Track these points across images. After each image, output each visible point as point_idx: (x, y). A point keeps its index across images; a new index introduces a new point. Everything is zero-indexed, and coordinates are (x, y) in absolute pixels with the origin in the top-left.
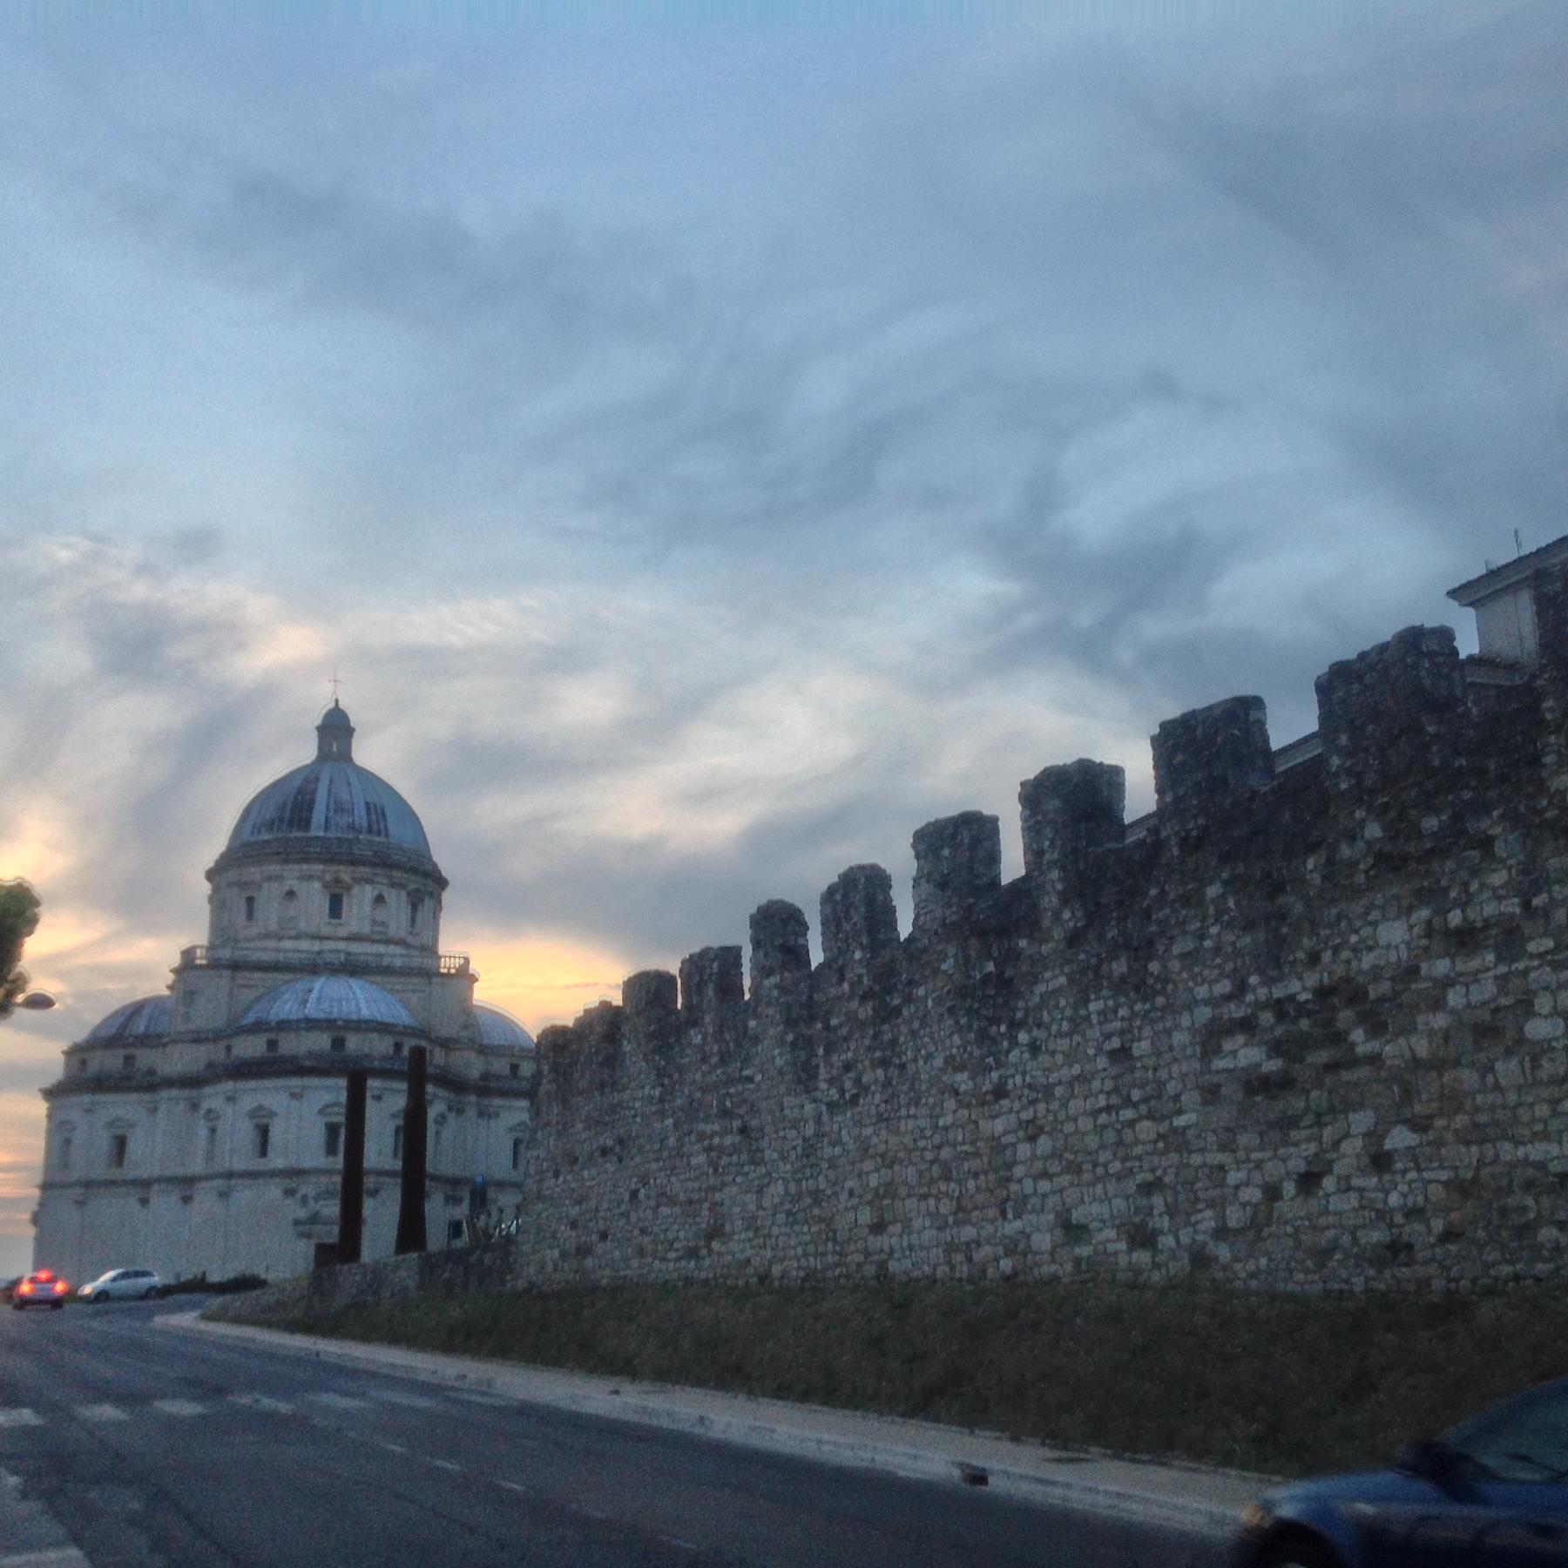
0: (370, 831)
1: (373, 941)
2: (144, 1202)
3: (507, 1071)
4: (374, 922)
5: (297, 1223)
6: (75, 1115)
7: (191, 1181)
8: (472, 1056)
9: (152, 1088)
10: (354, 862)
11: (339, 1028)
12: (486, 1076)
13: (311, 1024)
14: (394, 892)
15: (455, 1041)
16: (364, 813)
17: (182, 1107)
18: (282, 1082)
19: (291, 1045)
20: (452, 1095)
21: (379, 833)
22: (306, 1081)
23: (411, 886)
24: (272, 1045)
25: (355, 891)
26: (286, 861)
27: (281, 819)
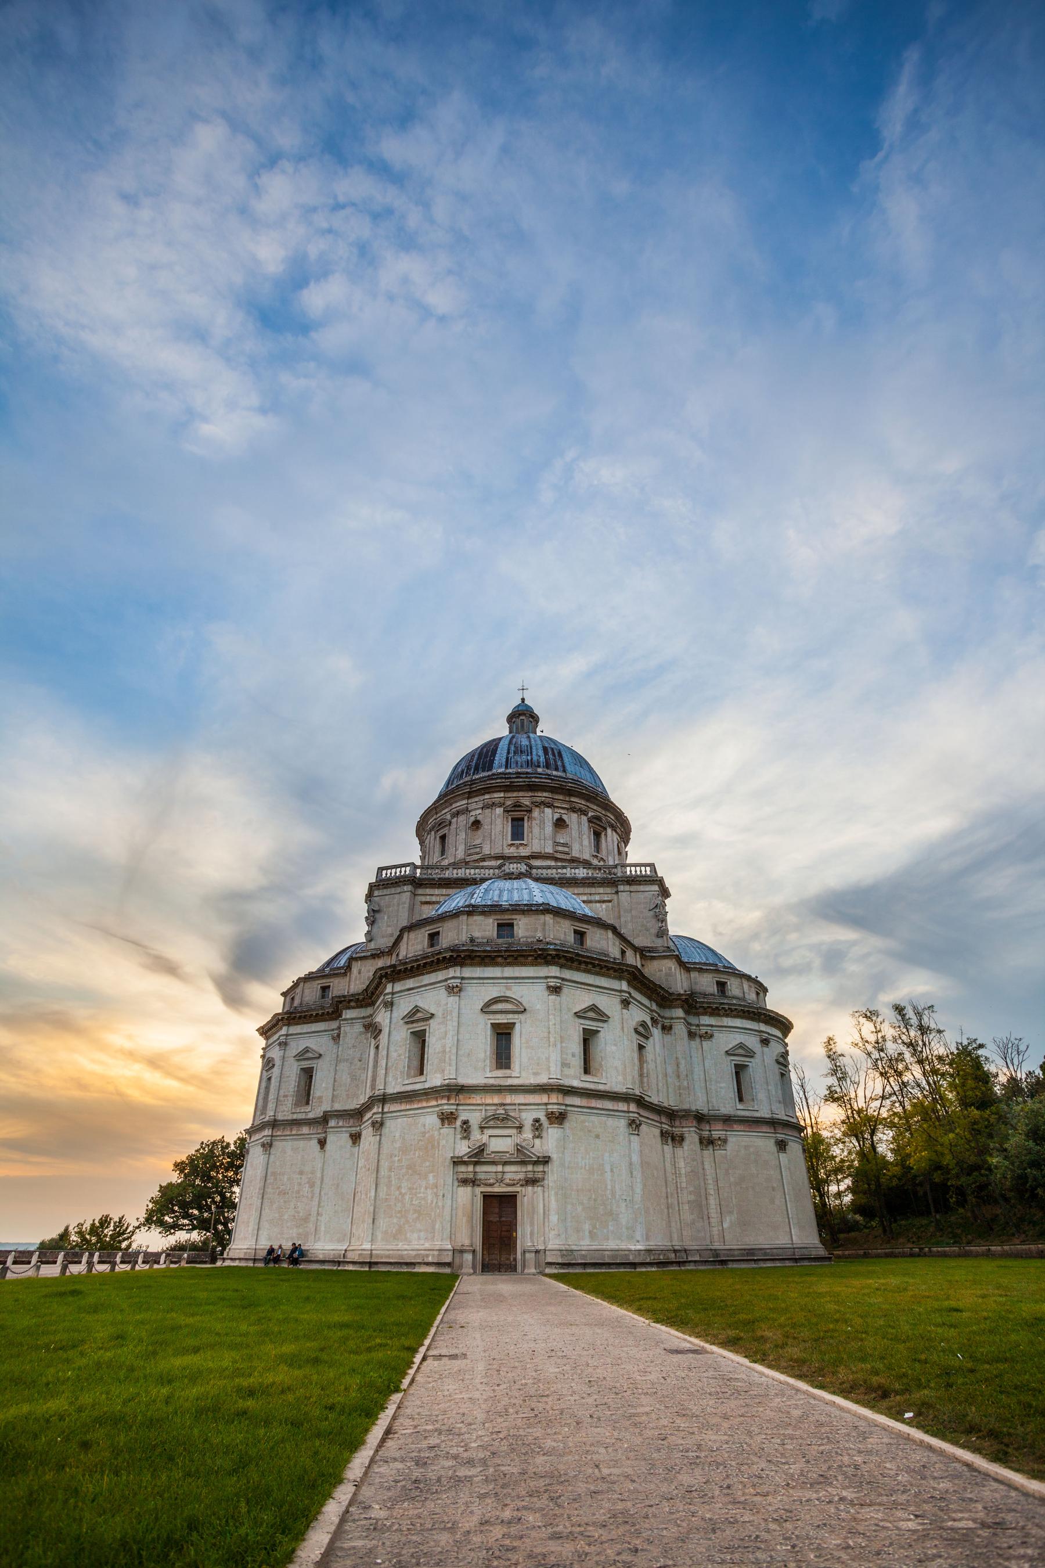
0: (547, 768)
1: (556, 859)
2: (322, 1143)
3: (714, 989)
4: (557, 844)
5: (457, 1162)
6: (276, 1053)
7: (358, 1114)
8: (671, 965)
10: (532, 788)
11: (505, 911)
13: (472, 911)
14: (574, 816)
15: (651, 950)
16: (541, 753)
17: (358, 1028)
18: (440, 975)
19: (452, 935)
20: (654, 1007)
21: (557, 769)
22: (468, 972)
23: (590, 814)
24: (433, 937)
25: (536, 813)
26: (470, 795)
27: (468, 768)
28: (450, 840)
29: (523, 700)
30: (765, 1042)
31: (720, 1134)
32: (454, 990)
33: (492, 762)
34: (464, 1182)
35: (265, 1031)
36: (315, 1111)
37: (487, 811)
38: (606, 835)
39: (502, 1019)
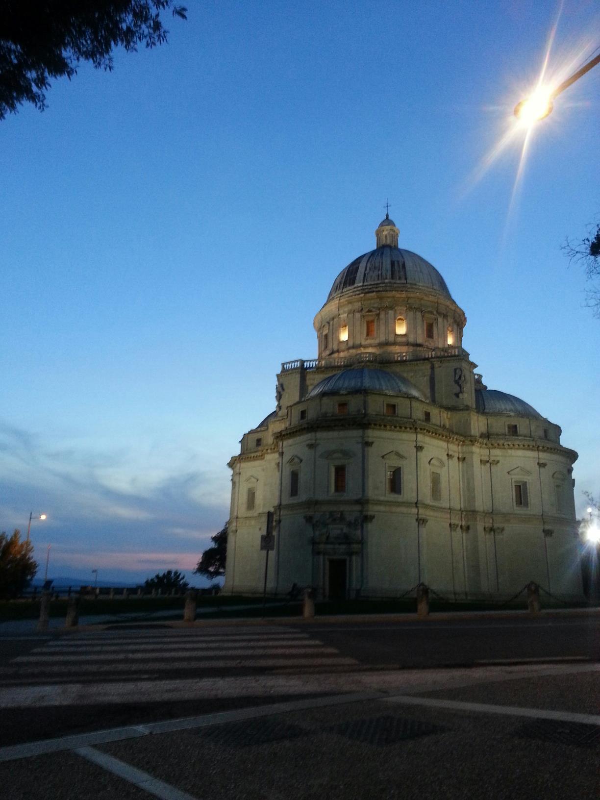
9: (262, 457)
12: (487, 436)
14: (411, 314)
16: (389, 267)
21: (400, 278)
22: (319, 435)
25: (382, 316)
27: (340, 283)
28: (330, 339)
29: (387, 216)
30: (542, 465)
31: (501, 526)
32: (311, 446)
33: (355, 278)
34: (319, 553)
35: (231, 465)
36: (255, 513)
37: (351, 315)
38: (437, 323)
39: (339, 463)
